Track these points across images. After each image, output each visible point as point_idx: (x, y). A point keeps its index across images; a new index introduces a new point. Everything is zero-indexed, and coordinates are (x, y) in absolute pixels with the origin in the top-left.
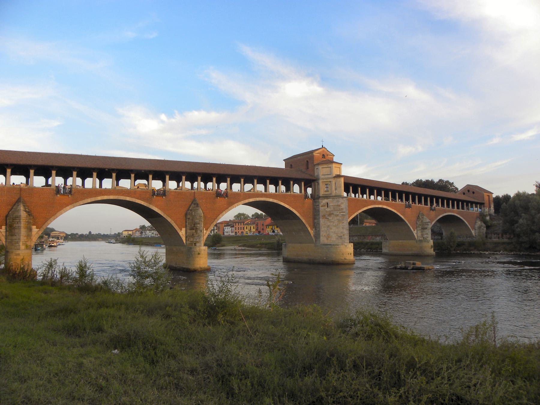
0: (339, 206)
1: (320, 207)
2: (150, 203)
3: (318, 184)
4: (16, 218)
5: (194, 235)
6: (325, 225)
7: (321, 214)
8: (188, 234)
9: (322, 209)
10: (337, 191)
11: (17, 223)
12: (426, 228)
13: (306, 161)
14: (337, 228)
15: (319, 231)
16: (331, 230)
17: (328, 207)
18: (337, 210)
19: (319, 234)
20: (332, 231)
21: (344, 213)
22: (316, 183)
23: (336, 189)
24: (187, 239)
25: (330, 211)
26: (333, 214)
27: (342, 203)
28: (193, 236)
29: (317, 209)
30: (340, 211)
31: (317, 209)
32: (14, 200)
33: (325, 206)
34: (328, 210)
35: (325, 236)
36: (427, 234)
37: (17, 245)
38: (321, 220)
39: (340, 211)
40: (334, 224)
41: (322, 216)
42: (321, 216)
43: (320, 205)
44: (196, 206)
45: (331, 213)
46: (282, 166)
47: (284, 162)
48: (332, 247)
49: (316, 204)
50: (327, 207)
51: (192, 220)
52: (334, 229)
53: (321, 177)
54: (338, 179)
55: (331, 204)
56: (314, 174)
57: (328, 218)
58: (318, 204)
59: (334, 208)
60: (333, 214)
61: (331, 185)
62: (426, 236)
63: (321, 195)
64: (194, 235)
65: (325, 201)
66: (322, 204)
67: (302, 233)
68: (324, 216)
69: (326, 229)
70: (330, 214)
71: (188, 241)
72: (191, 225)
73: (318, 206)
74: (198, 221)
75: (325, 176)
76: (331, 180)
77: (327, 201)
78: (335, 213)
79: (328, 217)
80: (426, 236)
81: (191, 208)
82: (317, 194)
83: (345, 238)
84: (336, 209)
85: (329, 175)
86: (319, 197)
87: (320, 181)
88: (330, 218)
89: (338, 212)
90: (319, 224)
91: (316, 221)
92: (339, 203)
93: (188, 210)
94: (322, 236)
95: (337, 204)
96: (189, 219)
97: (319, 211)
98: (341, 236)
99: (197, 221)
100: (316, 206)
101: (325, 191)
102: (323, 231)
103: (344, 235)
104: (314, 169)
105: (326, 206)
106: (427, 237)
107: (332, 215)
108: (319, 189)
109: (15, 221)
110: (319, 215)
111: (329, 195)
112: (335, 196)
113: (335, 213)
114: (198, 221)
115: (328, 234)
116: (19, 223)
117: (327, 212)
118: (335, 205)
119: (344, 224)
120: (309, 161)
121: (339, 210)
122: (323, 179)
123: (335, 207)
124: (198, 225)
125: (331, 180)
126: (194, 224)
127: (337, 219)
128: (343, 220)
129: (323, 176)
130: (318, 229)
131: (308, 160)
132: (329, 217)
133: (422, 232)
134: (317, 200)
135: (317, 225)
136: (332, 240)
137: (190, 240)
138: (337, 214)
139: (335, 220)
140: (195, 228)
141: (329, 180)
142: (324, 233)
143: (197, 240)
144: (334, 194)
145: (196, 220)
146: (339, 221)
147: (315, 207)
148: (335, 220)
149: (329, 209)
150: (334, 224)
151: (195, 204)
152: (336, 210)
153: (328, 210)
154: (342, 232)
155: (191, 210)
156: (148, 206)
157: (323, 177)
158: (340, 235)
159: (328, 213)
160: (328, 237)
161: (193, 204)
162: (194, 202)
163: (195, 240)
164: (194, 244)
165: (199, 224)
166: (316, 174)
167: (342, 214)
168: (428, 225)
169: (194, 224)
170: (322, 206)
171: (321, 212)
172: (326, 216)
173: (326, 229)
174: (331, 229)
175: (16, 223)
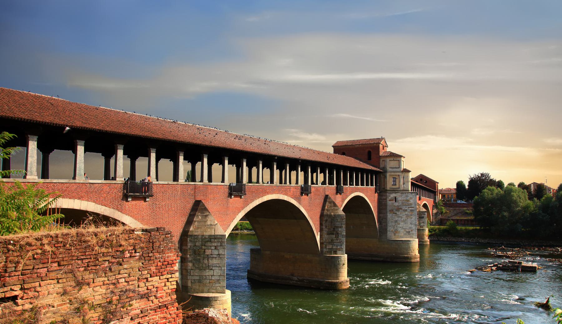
0: (408, 201)
1: (388, 201)
2: (300, 203)
3: (385, 177)
4: (213, 240)
5: (334, 241)
6: (392, 220)
7: (389, 208)
8: (324, 239)
9: (389, 203)
10: (405, 185)
11: (216, 249)
12: (423, 218)
13: (367, 151)
14: (405, 223)
15: (386, 225)
16: (399, 226)
17: (395, 201)
18: (406, 205)
19: (386, 230)
20: (400, 226)
21: (413, 209)
22: (382, 176)
23: (404, 184)
24: (324, 246)
25: (398, 206)
26: (401, 209)
27: (411, 198)
28: (332, 242)
29: (383, 203)
30: (409, 206)
31: (383, 203)
32: (190, 206)
33: (393, 200)
34: (396, 204)
35: (392, 231)
36: (423, 223)
37: (217, 285)
38: (388, 214)
39: (409, 206)
40: (402, 219)
41: (390, 211)
42: (388, 211)
43: (388, 199)
44: (332, 204)
45: (400, 207)
46: (331, 151)
47: (332, 149)
48: (403, 243)
49: (382, 198)
50: (394, 202)
51: (331, 222)
52: (402, 225)
53: (389, 169)
54: (406, 174)
55: (399, 199)
56: (379, 166)
57: (396, 213)
58: (385, 198)
59: (402, 203)
60: (401, 209)
61: (399, 179)
62: (422, 224)
63: (388, 189)
64: (334, 241)
65: (393, 195)
66: (390, 198)
67: (364, 227)
68: (391, 211)
69: (393, 224)
70: (398, 209)
71: (326, 248)
72: (329, 229)
73: (385, 200)
74: (339, 223)
75: (393, 169)
76: (399, 174)
77: (396, 195)
78: (404, 208)
79: (395, 212)
80: (422, 224)
81: (326, 208)
82: (382, 187)
83: (413, 234)
84: (405, 204)
85: (398, 169)
86: (387, 190)
87: (388, 174)
88: (398, 213)
89: (406, 208)
90: (386, 219)
91: (381, 215)
92: (408, 198)
93: (323, 209)
94: (390, 231)
95: (405, 199)
96: (326, 221)
97: (386, 205)
98: (409, 232)
99: (338, 224)
100: (381, 199)
101: (392, 185)
102: (390, 226)
103: (412, 231)
104: (379, 161)
105: (394, 200)
106: (424, 226)
107: (400, 210)
108: (385, 183)
109: (209, 244)
110: (386, 209)
111: (397, 189)
112: (403, 190)
113: (404, 208)
114: (339, 223)
115: (396, 229)
116: (219, 248)
117: (395, 206)
118: (404, 200)
119: (413, 219)
120: (371, 151)
121: (408, 205)
122: (391, 172)
123: (403, 202)
124: (340, 229)
125: (399, 174)
126: (334, 229)
127: (405, 214)
128: (412, 215)
129: (391, 169)
130: (384, 224)
131: (371, 150)
132: (396, 212)
133: (419, 220)
134: (384, 194)
135: (382, 220)
136: (400, 235)
137: (328, 247)
138: (406, 209)
139: (403, 215)
140: (335, 232)
141: (397, 174)
142: (391, 228)
143: (339, 247)
144: (402, 188)
145: (337, 223)
146: (407, 216)
147: (381, 200)
148: (403, 215)
149: (398, 204)
150: (402, 219)
151: (330, 202)
152: (404, 205)
153: (396, 204)
154: (410, 228)
155: (327, 210)
156: (298, 207)
157: (390, 170)
158: (408, 231)
159: (396, 208)
160: (396, 232)
161: (327, 203)
162: (328, 200)
163: (335, 247)
164: (334, 252)
165: (340, 228)
166: (382, 166)
167: (410, 209)
168: (425, 214)
169: (334, 229)
170: (390, 200)
171: (388, 207)
172: (394, 211)
173: (393, 224)
174: (399, 224)
175: (213, 248)
